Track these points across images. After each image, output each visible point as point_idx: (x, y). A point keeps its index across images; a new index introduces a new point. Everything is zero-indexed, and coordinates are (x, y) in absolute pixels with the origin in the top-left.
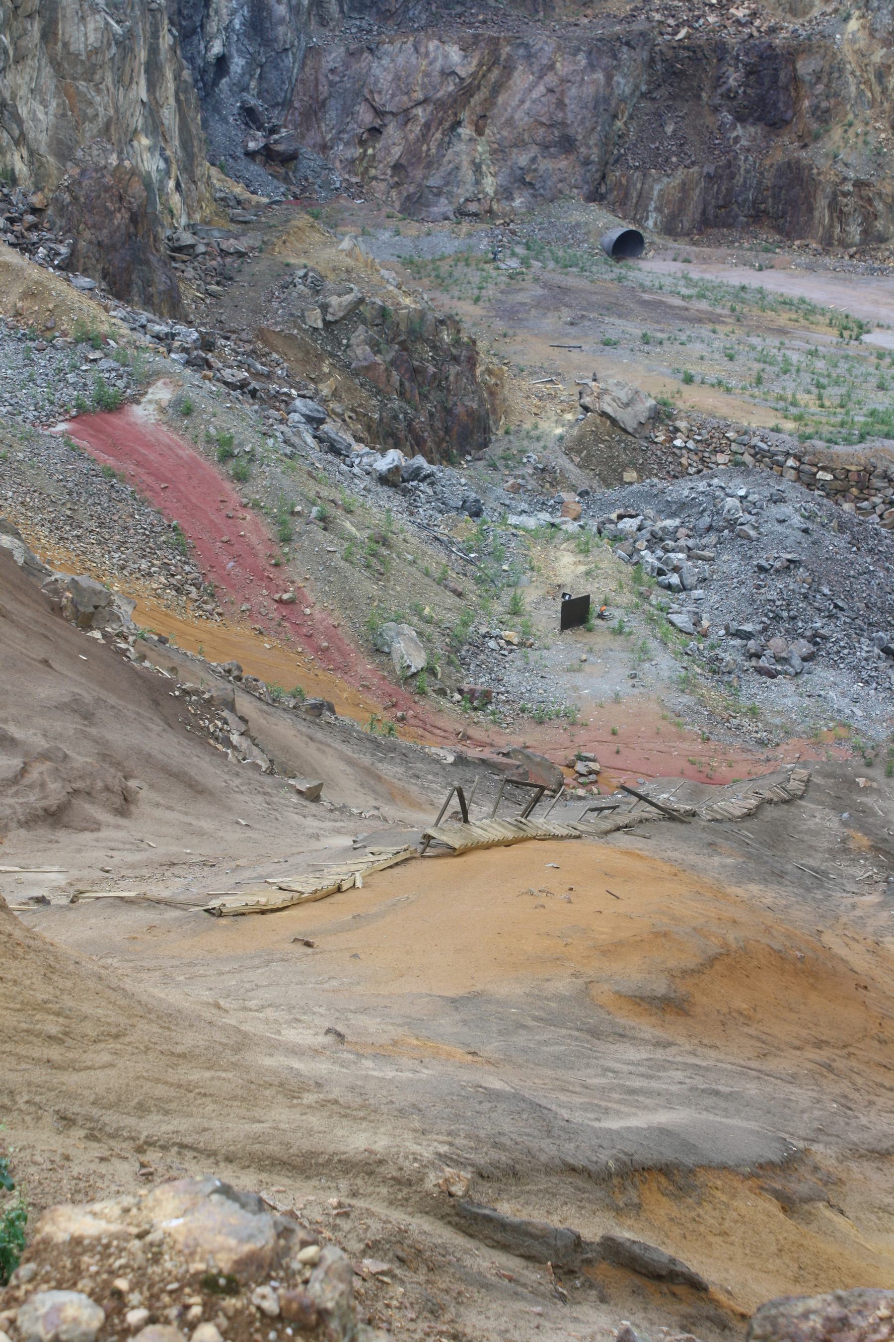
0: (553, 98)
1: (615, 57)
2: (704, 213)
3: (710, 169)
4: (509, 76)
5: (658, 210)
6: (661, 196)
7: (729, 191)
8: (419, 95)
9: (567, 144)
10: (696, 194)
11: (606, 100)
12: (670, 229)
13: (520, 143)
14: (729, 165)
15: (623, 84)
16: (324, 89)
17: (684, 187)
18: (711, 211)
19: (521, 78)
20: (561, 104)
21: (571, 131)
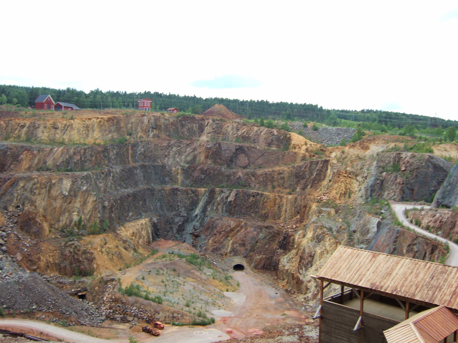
0: (244, 235)
1: (261, 230)
2: (264, 266)
3: (268, 257)
4: (242, 229)
5: (255, 263)
6: (256, 260)
7: (270, 263)
8: (223, 229)
9: (244, 245)
10: (263, 262)
11: (255, 238)
12: (255, 267)
13: (236, 243)
14: (272, 257)
15: (261, 235)
16: (210, 225)
17: (261, 259)
18: (265, 266)
19: (243, 230)
20: (245, 237)
21: (245, 242)
